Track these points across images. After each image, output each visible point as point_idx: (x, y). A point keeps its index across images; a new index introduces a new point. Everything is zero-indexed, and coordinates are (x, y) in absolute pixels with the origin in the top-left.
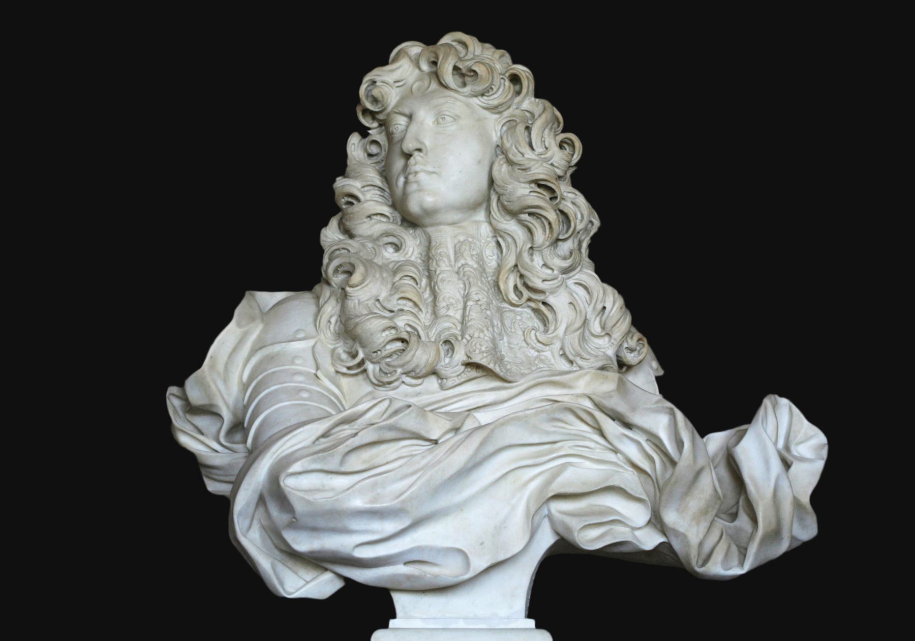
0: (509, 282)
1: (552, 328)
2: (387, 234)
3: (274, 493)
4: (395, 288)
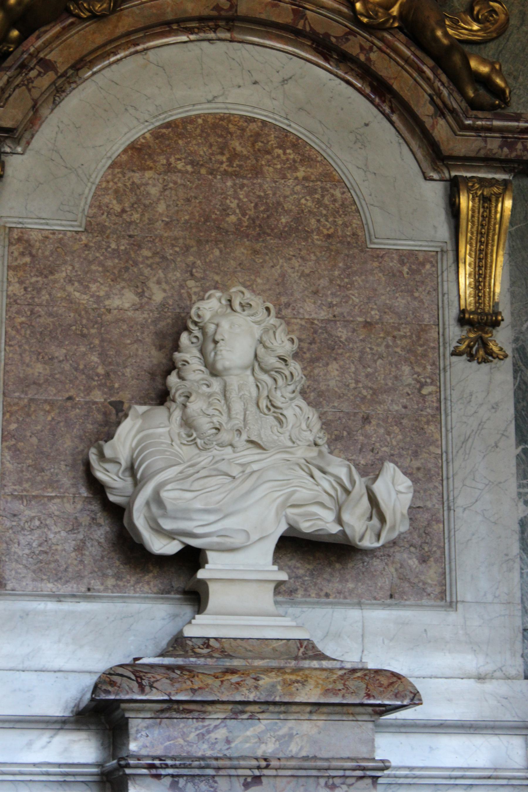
0: (264, 403)
1: (285, 425)
2: (203, 379)
3: (157, 499)
4: (210, 404)
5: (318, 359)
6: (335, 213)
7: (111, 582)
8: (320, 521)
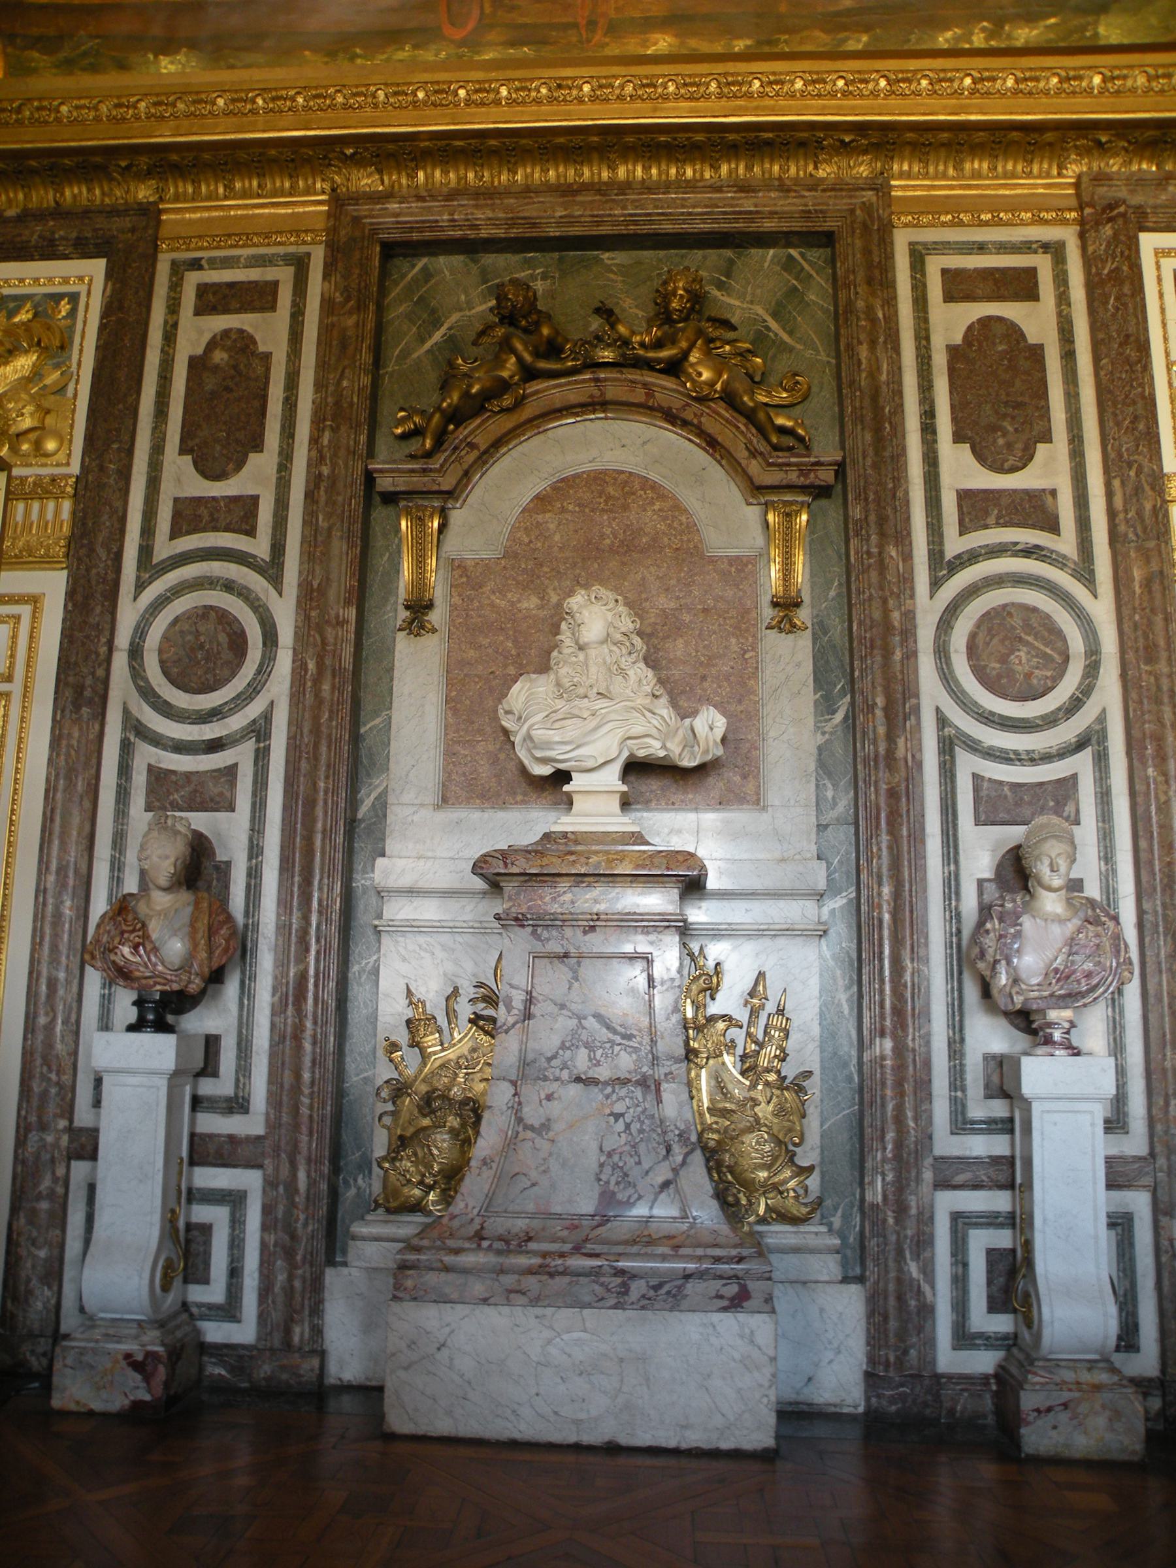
5: (668, 637)
6: (682, 533)
7: (519, 798)
8: (653, 749)
